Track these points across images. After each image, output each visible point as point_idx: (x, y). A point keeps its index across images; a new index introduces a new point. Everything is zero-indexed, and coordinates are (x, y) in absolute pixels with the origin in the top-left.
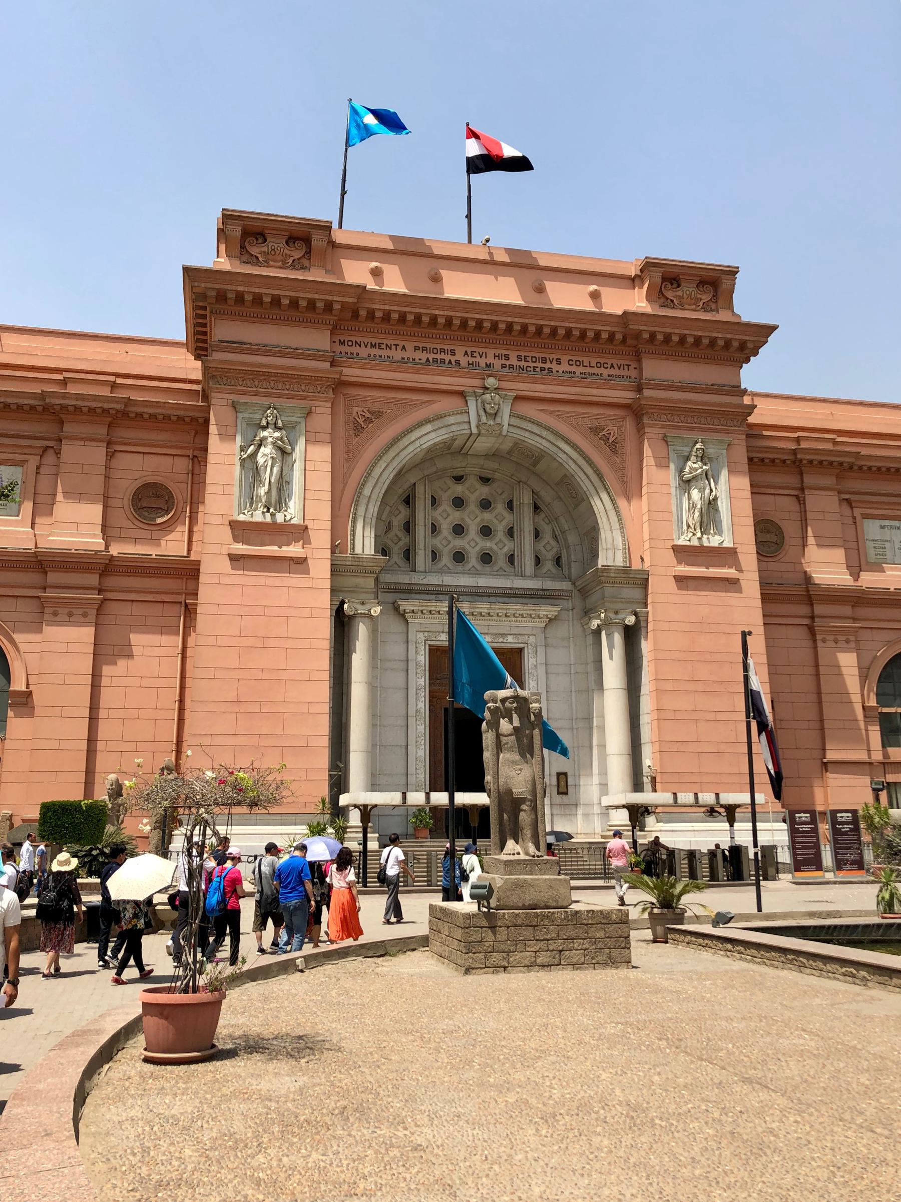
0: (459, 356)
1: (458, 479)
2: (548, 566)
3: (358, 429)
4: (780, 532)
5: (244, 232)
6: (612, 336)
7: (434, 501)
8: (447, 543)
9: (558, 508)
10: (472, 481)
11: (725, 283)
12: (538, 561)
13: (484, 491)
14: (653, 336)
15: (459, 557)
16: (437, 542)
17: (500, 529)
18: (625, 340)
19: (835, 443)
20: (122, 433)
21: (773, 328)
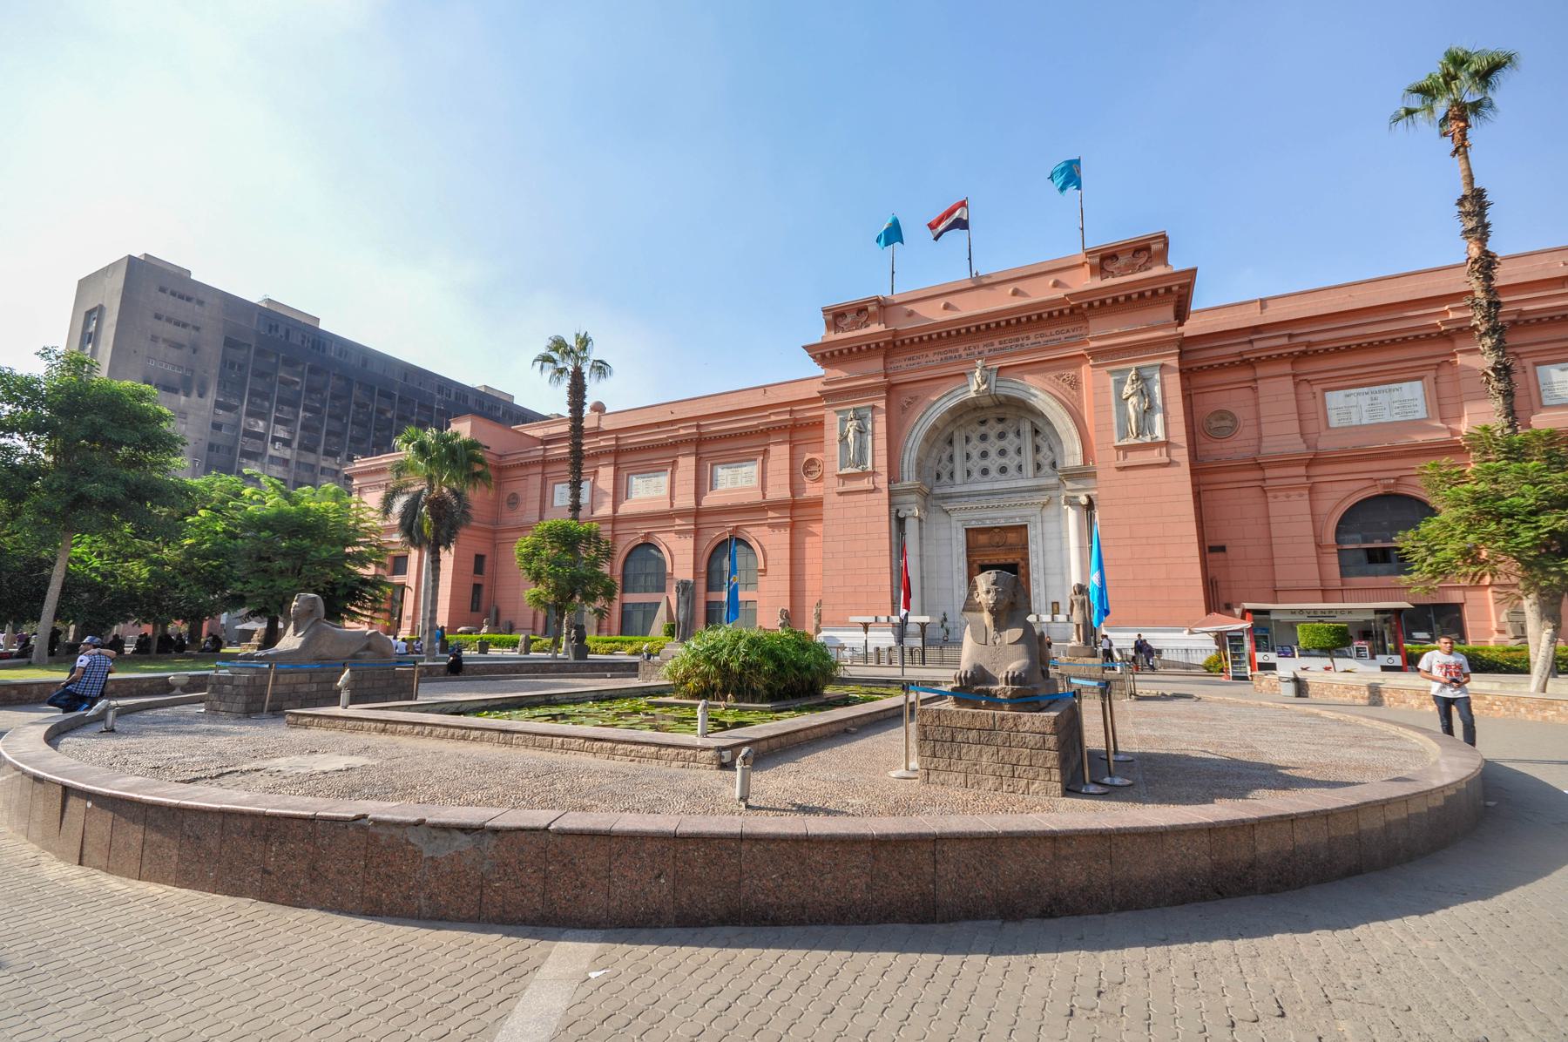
0: (961, 352)
1: (983, 423)
2: (1046, 469)
3: (904, 409)
4: (1234, 419)
5: (836, 317)
6: (1061, 312)
7: (968, 440)
8: (976, 464)
9: (1047, 430)
10: (992, 422)
11: (1155, 247)
12: (1039, 467)
13: (1000, 427)
14: (1091, 304)
15: (985, 472)
16: (969, 465)
17: (1011, 451)
18: (1077, 311)
19: (1290, 336)
20: (797, 436)
21: (1195, 270)
